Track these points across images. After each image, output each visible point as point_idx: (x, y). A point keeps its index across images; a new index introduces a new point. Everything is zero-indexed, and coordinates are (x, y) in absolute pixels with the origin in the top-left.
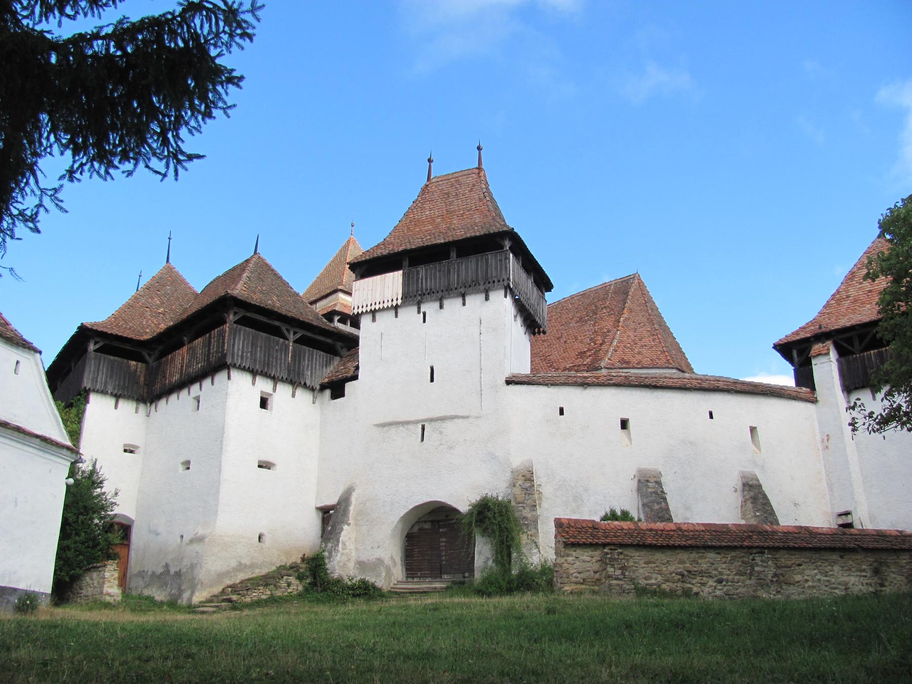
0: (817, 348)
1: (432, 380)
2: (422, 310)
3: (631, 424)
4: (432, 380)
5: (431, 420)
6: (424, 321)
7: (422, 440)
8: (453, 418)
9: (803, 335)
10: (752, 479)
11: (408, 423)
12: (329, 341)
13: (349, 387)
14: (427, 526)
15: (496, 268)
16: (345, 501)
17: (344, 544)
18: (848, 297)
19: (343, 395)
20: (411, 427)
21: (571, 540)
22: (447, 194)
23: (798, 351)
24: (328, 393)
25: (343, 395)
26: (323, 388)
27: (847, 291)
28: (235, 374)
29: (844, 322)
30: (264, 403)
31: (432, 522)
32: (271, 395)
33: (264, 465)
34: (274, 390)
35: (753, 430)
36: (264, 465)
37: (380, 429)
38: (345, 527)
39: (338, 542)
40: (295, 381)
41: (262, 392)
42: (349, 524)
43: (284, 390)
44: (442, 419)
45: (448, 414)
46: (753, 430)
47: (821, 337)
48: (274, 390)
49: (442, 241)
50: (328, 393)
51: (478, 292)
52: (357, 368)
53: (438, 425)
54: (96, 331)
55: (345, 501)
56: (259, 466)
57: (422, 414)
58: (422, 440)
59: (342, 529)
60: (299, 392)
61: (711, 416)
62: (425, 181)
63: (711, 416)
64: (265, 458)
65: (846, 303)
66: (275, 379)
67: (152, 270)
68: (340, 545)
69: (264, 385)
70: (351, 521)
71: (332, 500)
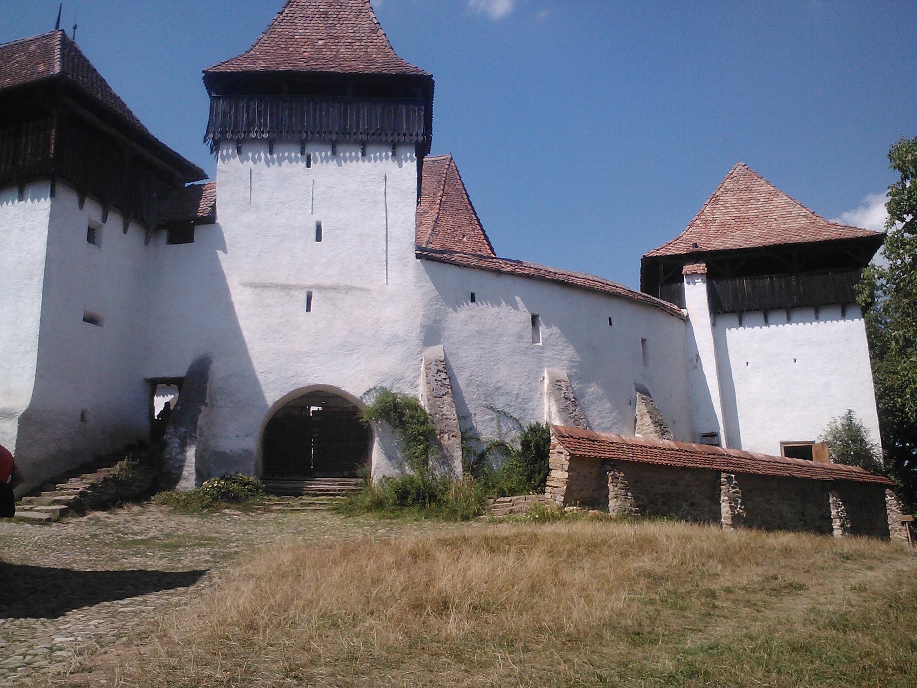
0: (687, 269)
1: (319, 238)
2: (309, 150)
4: (319, 238)
5: (320, 288)
6: (308, 166)
7: (308, 309)
8: (350, 289)
9: (673, 251)
11: (286, 287)
13: (200, 232)
15: (408, 119)
17: (201, 429)
22: (326, 13)
24: (164, 234)
26: (159, 227)
27: (713, 214)
28: (60, 190)
29: (718, 244)
30: (92, 235)
32: (99, 226)
33: (90, 319)
34: (104, 219)
36: (90, 319)
37: (249, 291)
38: (203, 408)
39: (195, 427)
41: (90, 219)
42: (206, 405)
43: (114, 222)
44: (334, 288)
45: (342, 283)
47: (695, 256)
48: (104, 219)
50: (164, 234)
51: (381, 143)
52: (214, 207)
53: (331, 294)
56: (84, 320)
57: (310, 282)
58: (308, 309)
59: (200, 412)
60: (133, 228)
64: (94, 309)
66: (106, 207)
69: (92, 212)
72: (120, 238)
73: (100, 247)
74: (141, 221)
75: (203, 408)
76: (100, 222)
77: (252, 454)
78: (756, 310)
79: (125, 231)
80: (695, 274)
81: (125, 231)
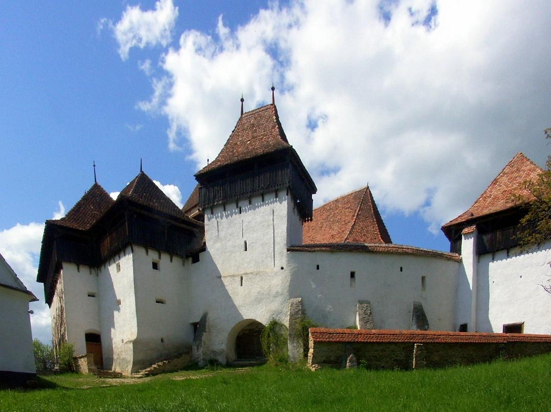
0: (466, 230)
3: (356, 275)
9: (460, 221)
10: (419, 306)
12: (189, 227)
13: (201, 255)
14: (247, 332)
16: (204, 318)
17: (205, 342)
18: (490, 195)
19: (198, 260)
20: (236, 278)
21: (318, 340)
23: (454, 232)
25: (198, 260)
30: (155, 266)
31: (250, 330)
34: (160, 258)
35: (423, 278)
39: (201, 340)
40: (172, 253)
42: (206, 332)
43: (165, 258)
46: (423, 278)
47: (468, 223)
48: (160, 258)
49: (249, 157)
52: (205, 243)
54: (56, 225)
55: (204, 318)
56: (157, 302)
59: (203, 335)
60: (175, 259)
61: (401, 270)
62: (240, 116)
63: (401, 270)
64: (159, 298)
65: (489, 200)
67: (86, 186)
68: (203, 343)
70: (207, 330)
71: (197, 320)
72: (170, 265)
73: (159, 270)
74: (177, 255)
75: (204, 334)
76: (158, 259)
77: (224, 351)
78: (502, 249)
79: (171, 260)
80: (468, 235)
81: (171, 260)
